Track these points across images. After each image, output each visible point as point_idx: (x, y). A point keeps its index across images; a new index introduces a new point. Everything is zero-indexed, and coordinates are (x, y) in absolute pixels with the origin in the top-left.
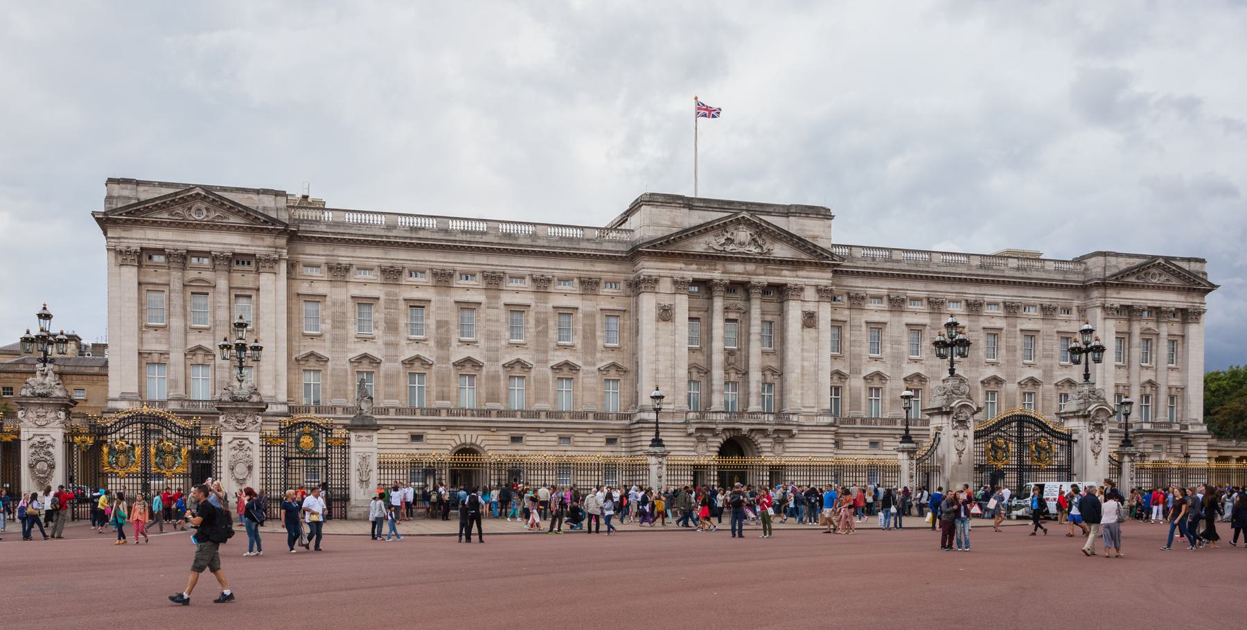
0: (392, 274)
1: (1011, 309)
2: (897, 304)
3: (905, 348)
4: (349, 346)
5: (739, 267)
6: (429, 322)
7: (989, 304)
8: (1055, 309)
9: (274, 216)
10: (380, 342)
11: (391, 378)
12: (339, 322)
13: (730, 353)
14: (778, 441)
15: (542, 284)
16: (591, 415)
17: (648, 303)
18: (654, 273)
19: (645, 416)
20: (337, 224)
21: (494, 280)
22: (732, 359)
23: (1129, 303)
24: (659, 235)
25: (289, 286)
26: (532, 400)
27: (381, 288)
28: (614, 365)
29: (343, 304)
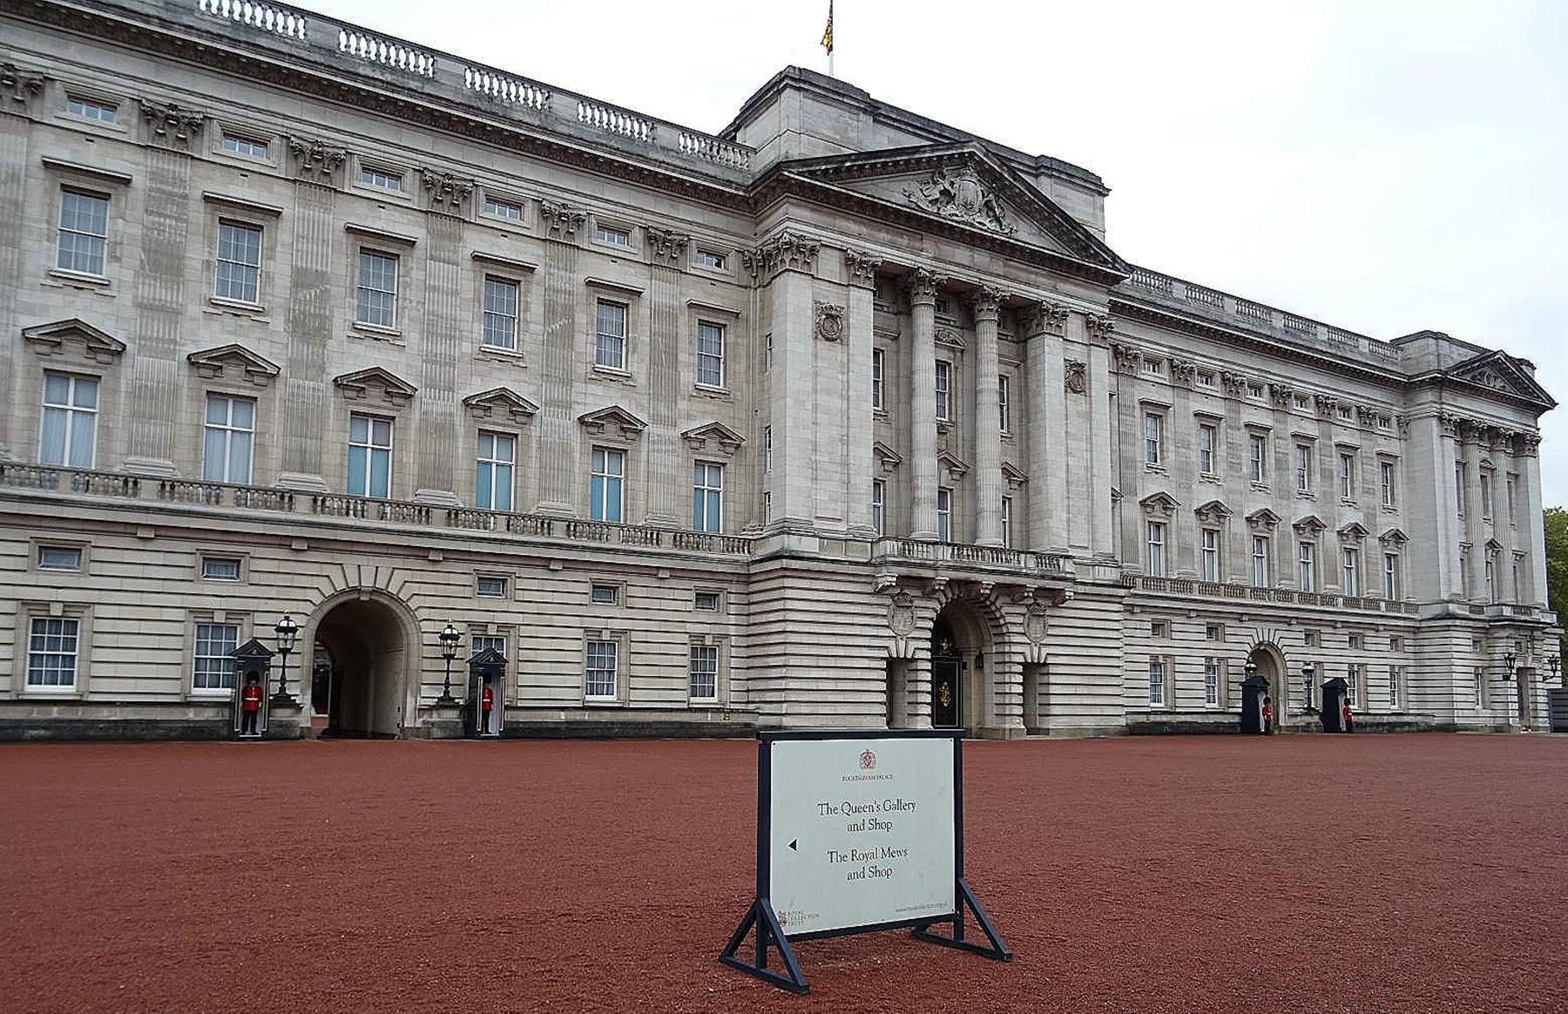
2: (1181, 374)
3: (1195, 457)
4: (24, 296)
5: (961, 254)
6: (271, 266)
8: (1374, 415)
10: (126, 298)
11: (149, 400)
14: (1035, 613)
16: (667, 538)
17: (796, 297)
19: (792, 543)
23: (1465, 415)
26: (532, 492)
27: (140, 159)
28: (716, 431)
29: (13, 177)
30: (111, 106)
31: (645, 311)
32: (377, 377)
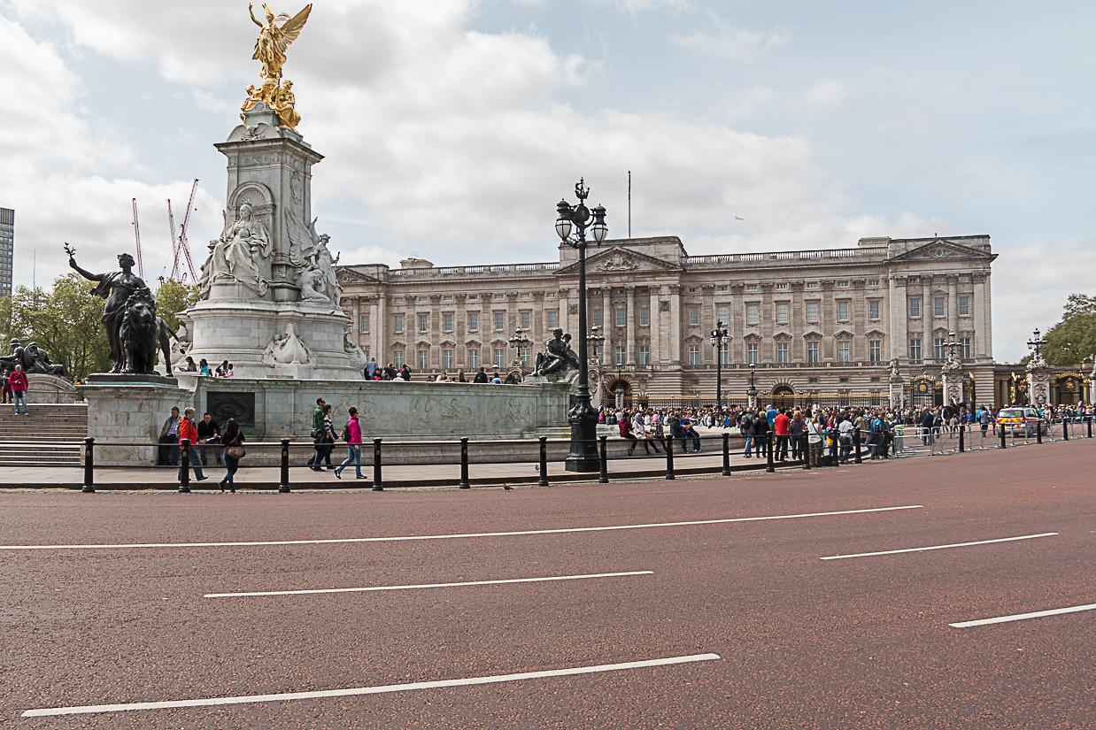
0: (436, 299)
1: (827, 286)
2: (738, 290)
3: (745, 318)
4: (416, 338)
5: (617, 279)
7: (808, 284)
8: (864, 282)
9: (376, 277)
12: (411, 326)
13: (620, 329)
15: (512, 298)
18: (566, 287)
20: (410, 276)
21: (487, 298)
22: (620, 333)
24: (569, 265)
25: (387, 311)
30: (425, 298)
31: (533, 313)
32: (472, 342)
